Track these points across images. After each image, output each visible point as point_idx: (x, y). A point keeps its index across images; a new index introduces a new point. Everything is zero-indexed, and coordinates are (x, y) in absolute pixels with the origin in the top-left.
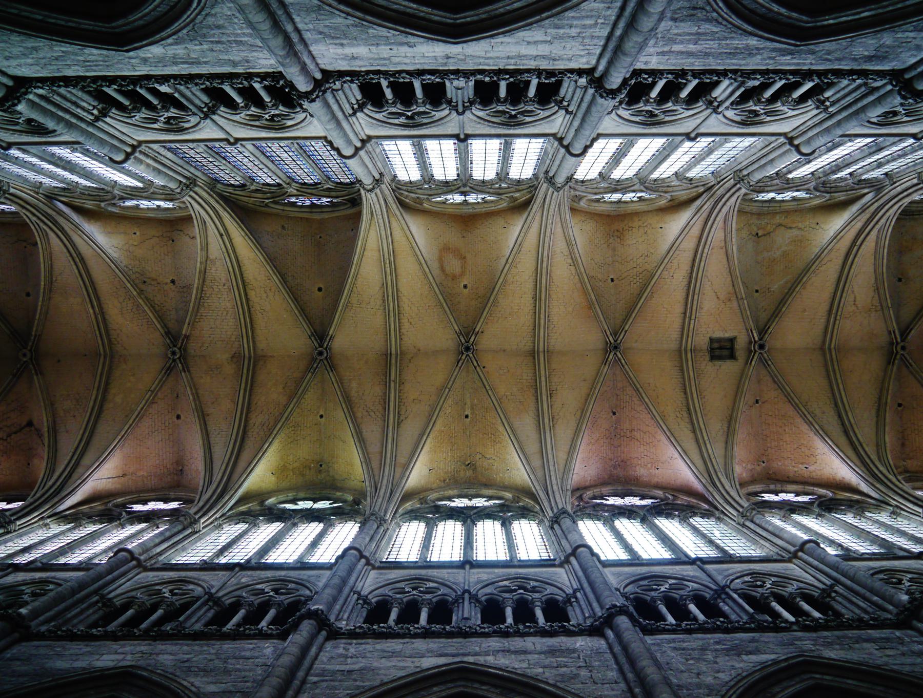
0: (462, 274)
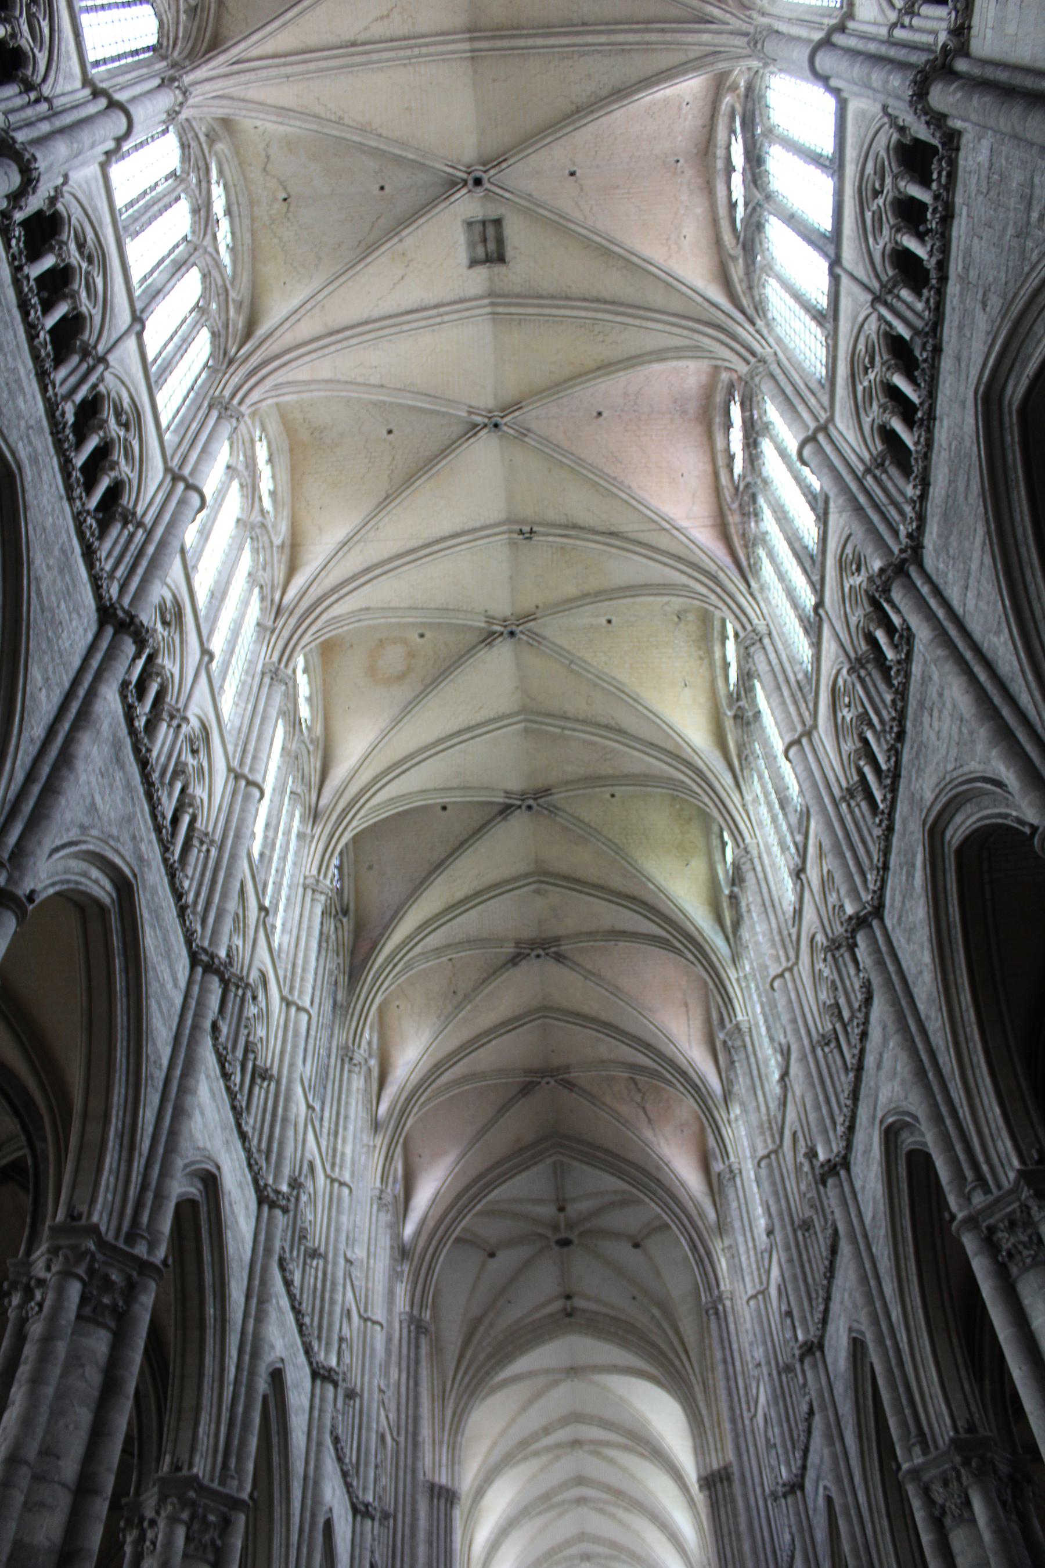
0: (405, 642)
